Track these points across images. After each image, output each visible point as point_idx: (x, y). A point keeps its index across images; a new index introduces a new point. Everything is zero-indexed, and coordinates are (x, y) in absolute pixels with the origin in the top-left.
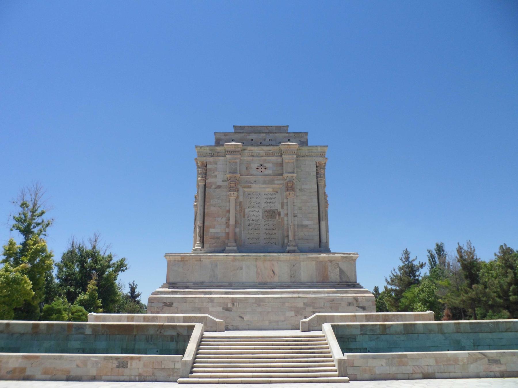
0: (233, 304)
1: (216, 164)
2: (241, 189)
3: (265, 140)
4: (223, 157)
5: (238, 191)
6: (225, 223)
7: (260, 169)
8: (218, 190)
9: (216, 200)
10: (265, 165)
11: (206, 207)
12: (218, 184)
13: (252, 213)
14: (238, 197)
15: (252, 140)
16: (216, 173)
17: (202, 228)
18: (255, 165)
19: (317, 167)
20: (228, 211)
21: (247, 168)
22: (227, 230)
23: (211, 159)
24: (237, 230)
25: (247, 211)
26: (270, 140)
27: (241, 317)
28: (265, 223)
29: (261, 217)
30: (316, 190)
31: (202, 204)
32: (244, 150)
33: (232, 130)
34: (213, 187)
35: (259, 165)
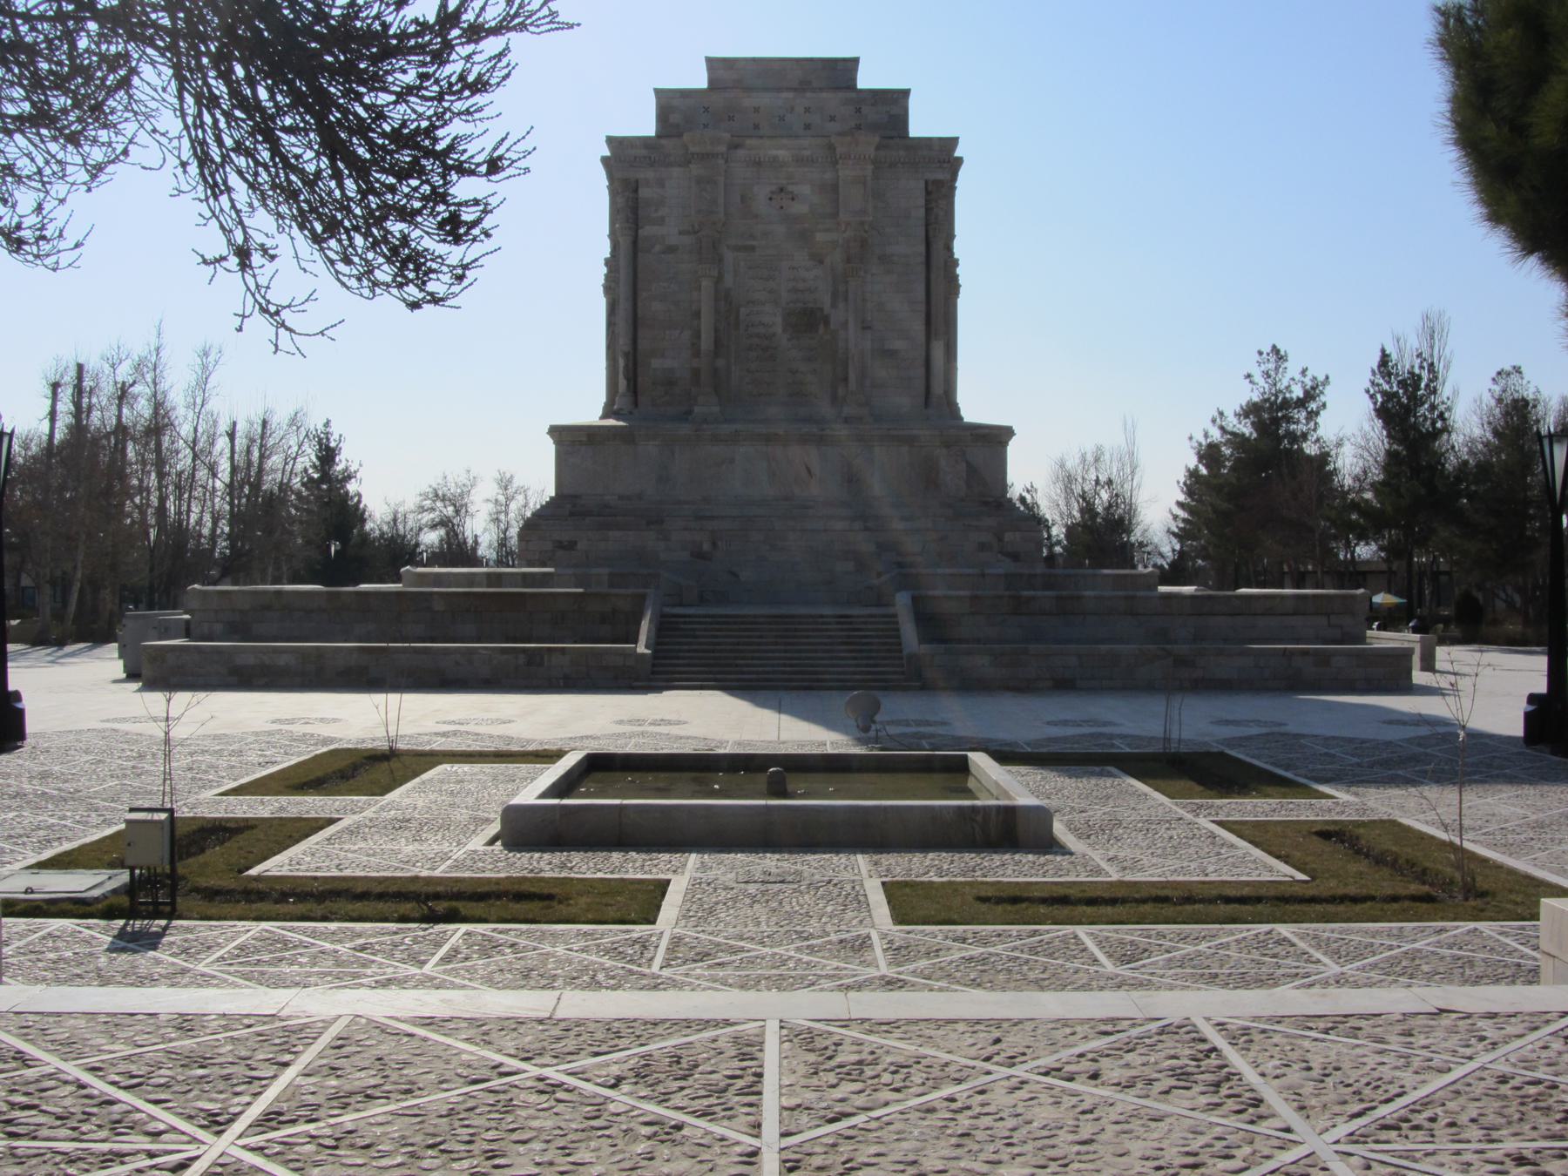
0: (714, 544)
1: (662, 186)
2: (729, 256)
3: (792, 109)
5: (721, 260)
10: (790, 188)
11: (640, 304)
14: (719, 280)
15: (757, 110)
18: (761, 192)
19: (928, 193)
20: (697, 314)
21: (743, 199)
23: (650, 174)
24: (721, 363)
26: (807, 110)
27: (735, 575)
29: (779, 329)
30: (922, 259)
32: (737, 147)
33: (700, 81)
34: (658, 248)
35: (774, 188)
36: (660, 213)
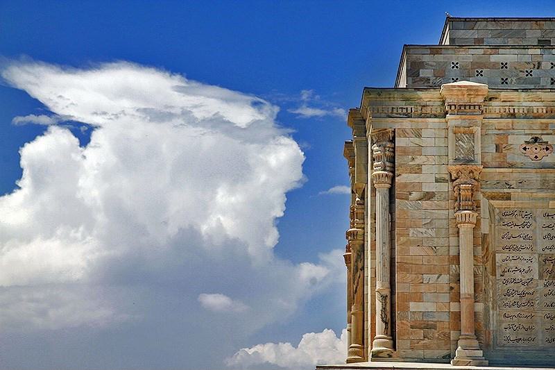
1: (419, 136)
2: (484, 203)
3: (539, 64)
4: (436, 116)
5: (478, 207)
6: (446, 288)
7: (534, 150)
8: (425, 204)
9: (423, 230)
10: (545, 138)
12: (426, 189)
13: (512, 264)
15: (504, 65)
16: (419, 160)
17: (388, 300)
20: (457, 259)
22: (454, 307)
24: (480, 307)
25: (499, 257)
28: (547, 290)
31: (387, 240)
34: (415, 195)
35: (529, 138)
36: (417, 162)
